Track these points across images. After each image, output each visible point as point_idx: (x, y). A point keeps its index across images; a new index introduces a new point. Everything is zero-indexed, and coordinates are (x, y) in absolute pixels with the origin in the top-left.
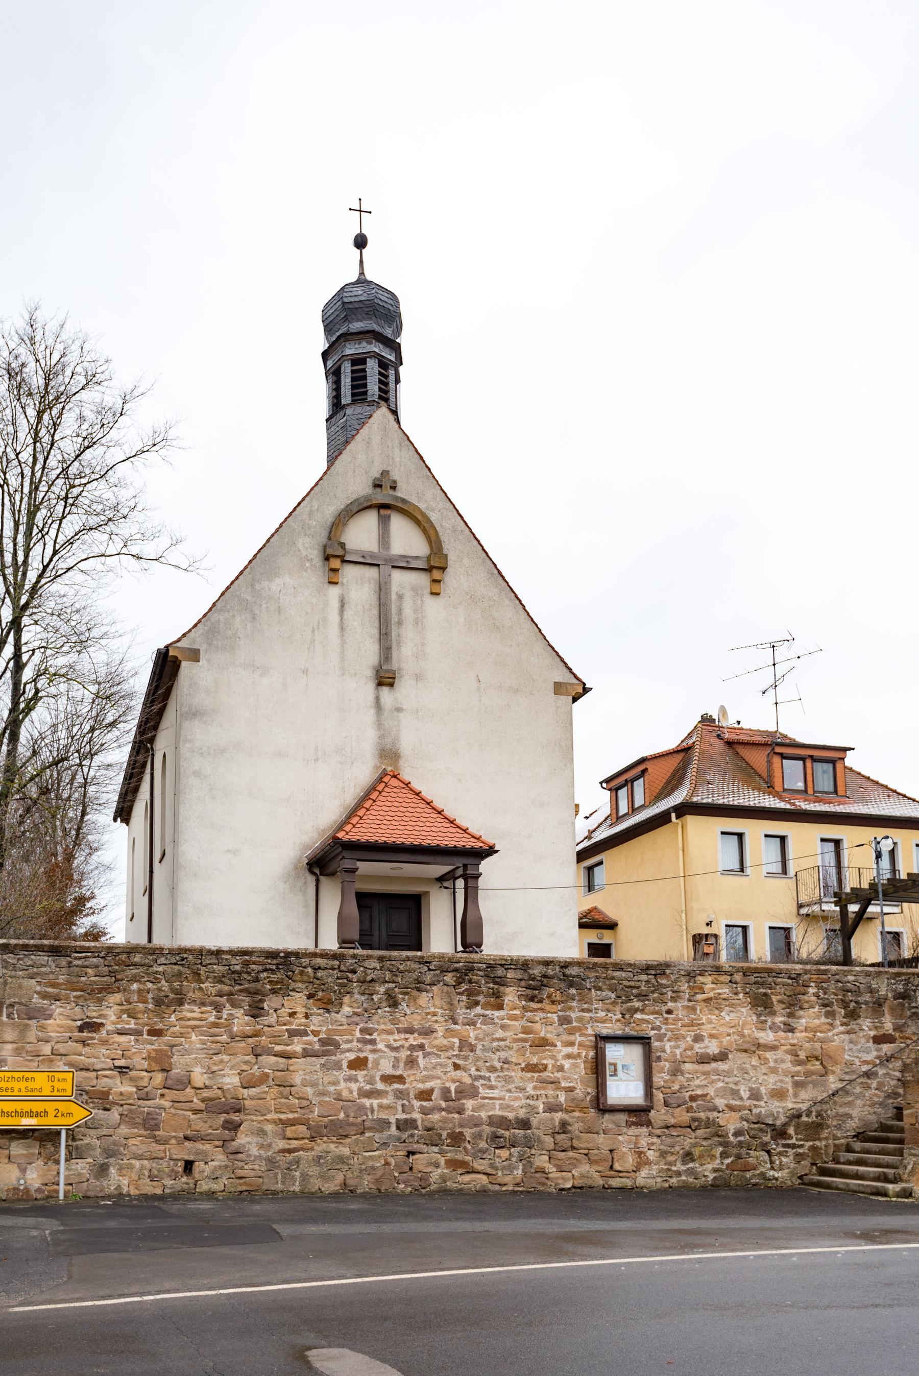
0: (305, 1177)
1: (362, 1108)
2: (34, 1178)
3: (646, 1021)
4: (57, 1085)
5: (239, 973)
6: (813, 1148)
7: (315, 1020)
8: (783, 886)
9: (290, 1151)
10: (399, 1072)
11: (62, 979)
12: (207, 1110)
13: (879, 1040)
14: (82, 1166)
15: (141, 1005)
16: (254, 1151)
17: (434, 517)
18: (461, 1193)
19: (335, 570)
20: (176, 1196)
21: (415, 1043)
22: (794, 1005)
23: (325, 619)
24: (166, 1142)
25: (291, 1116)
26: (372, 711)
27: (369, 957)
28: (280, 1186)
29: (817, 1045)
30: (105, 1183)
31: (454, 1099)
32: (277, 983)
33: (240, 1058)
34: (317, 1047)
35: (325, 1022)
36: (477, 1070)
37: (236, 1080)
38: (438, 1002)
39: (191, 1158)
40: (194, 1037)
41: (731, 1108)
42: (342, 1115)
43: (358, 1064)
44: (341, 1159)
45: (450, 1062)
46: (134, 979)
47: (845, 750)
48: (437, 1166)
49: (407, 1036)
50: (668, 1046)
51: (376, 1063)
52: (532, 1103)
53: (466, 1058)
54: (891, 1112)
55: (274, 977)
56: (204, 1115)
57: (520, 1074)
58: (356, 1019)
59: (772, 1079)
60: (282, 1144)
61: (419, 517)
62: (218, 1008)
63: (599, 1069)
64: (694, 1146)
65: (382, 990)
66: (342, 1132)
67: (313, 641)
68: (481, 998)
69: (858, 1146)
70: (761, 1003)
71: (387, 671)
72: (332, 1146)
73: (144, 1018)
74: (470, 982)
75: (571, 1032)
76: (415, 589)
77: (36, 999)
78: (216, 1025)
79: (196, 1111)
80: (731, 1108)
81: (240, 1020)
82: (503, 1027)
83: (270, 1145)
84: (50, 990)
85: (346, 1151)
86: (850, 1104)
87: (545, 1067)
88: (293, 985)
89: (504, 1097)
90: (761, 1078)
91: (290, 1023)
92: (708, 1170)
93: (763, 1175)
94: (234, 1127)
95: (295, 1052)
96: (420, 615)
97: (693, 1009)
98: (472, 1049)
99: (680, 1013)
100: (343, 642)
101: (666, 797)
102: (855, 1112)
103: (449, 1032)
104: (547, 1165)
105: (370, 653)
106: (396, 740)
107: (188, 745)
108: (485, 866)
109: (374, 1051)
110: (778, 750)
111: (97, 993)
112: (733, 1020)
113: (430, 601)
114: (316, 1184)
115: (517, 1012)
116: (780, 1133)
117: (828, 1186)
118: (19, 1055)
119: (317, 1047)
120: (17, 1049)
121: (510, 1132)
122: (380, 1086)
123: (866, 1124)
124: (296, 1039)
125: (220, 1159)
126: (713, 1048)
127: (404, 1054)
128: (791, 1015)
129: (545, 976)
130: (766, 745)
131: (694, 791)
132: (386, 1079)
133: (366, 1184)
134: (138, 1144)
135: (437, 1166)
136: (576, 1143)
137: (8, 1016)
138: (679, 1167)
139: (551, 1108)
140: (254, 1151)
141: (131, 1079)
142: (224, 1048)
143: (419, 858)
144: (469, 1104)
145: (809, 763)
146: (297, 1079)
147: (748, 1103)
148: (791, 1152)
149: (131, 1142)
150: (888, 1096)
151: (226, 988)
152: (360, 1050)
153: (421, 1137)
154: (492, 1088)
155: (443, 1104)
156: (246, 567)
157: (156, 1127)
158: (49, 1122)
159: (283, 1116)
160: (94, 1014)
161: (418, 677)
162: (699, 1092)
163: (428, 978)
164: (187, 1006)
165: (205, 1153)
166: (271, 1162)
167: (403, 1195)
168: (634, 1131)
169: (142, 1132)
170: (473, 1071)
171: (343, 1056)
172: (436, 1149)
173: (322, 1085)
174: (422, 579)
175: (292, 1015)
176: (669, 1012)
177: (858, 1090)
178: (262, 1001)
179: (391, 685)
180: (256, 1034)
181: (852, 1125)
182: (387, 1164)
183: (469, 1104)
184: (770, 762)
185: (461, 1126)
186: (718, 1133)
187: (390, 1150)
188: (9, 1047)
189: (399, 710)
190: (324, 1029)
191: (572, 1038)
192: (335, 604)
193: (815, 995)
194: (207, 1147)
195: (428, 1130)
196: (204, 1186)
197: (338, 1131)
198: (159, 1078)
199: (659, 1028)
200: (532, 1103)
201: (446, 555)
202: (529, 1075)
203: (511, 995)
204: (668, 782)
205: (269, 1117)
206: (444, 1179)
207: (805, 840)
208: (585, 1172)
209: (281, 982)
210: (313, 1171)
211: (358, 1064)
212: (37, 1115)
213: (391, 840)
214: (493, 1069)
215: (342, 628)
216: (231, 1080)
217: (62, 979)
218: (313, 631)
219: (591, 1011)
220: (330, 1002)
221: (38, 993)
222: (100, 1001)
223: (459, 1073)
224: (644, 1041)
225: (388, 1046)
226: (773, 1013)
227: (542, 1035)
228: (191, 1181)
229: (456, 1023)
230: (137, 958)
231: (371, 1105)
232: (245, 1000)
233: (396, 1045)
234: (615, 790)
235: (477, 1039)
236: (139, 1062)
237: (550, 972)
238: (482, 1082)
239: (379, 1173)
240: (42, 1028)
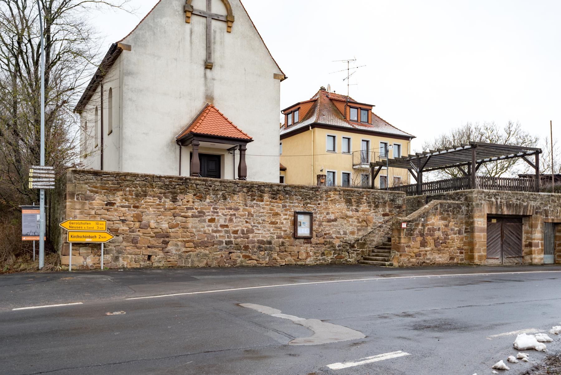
0: (193, 261)
1: (213, 236)
2: (90, 261)
3: (311, 207)
4: (100, 226)
5: (168, 185)
6: (362, 251)
8: (349, 157)
9: (187, 252)
10: (226, 224)
11: (98, 185)
12: (156, 236)
13: (384, 215)
14: (109, 257)
15: (130, 196)
16: (174, 252)
18: (247, 267)
19: (189, 17)
20: (146, 268)
22: (359, 203)
24: (141, 248)
25: (187, 239)
26: (203, 79)
27: (216, 181)
28: (183, 265)
29: (365, 216)
30: (118, 264)
31: (246, 233)
32: (182, 189)
33: (168, 217)
34: (197, 214)
35: (200, 205)
37: (167, 226)
38: (241, 198)
39: (151, 254)
41: (337, 238)
43: (212, 220)
44: (206, 255)
46: (127, 186)
47: (372, 106)
48: (239, 257)
50: (318, 216)
51: (218, 220)
53: (250, 219)
54: (386, 239)
55: (181, 187)
56: (155, 238)
57: (268, 225)
58: (211, 204)
59: (351, 228)
60: (184, 249)
62: (160, 198)
63: (295, 224)
64: (325, 250)
65: (221, 193)
66: (206, 245)
67: (179, 47)
68: (256, 197)
69: (376, 250)
70: (349, 202)
71: (209, 63)
72: (202, 250)
73: (131, 201)
74: (252, 191)
75: (286, 210)
76: (221, 29)
77: (88, 192)
78: (159, 205)
79: (152, 237)
80: (337, 238)
81: (168, 203)
82: (263, 208)
83: (180, 250)
84: (94, 189)
85: (207, 252)
86: (374, 236)
87: (277, 223)
88: (188, 191)
89: (263, 233)
90: (347, 227)
91: (187, 205)
92: (329, 259)
93: (346, 260)
94: (166, 243)
97: (327, 203)
99: (323, 205)
100: (191, 49)
101: (307, 119)
102: (375, 239)
103: (244, 210)
104: (277, 257)
105: (202, 54)
107: (126, 87)
108: (248, 145)
109: (218, 216)
110: (349, 104)
111: (113, 191)
112: (339, 207)
113: (227, 35)
114: (197, 264)
115: (268, 203)
116: (352, 246)
117: (367, 263)
118: (82, 214)
119: (197, 214)
120: (81, 212)
121: (265, 246)
122: (220, 229)
123: (379, 243)
124: (189, 211)
125: (161, 254)
126: (332, 217)
127: (228, 217)
128: (358, 206)
129: (278, 190)
130: (344, 102)
131: (318, 118)
132: (222, 226)
133: (215, 264)
134: (130, 249)
135: (239, 257)
136: (287, 249)
137: (77, 199)
138: (320, 258)
139: (279, 237)
140: (174, 252)
141: (127, 224)
142: (162, 214)
143: (224, 141)
144: (251, 235)
145: (359, 110)
146: (190, 225)
147: (343, 236)
148: (355, 252)
149: (127, 248)
150: (386, 234)
151: (163, 191)
152: (213, 215)
153: (234, 247)
154: (259, 230)
155: (242, 235)
156: (151, 12)
157: (137, 243)
158: (97, 240)
159: (184, 239)
161: (221, 67)
162: (327, 232)
163: (237, 189)
164: (148, 197)
165: (156, 253)
166: (180, 256)
167: (228, 267)
168: (306, 245)
169: (131, 244)
170: (252, 224)
172: (239, 251)
173: (199, 228)
174: (223, 25)
175: (188, 202)
176: (319, 204)
177: (377, 232)
178: (177, 196)
179: (211, 69)
180: (174, 209)
181: (375, 243)
182: (222, 256)
183: (251, 235)
184: (345, 109)
185: (248, 243)
186: (333, 246)
187: (223, 252)
188: (78, 211)
189: (214, 79)
191: (286, 213)
192: (188, 32)
193: (366, 199)
194: (156, 250)
195: (237, 244)
196: (155, 265)
197: (204, 245)
198: (137, 224)
199: (315, 210)
203: (266, 197)
204: (308, 113)
205: (179, 239)
206: (242, 262)
207: (357, 140)
208: (289, 259)
209: (184, 189)
210: (196, 259)
211: (212, 220)
212: (92, 237)
213: (213, 134)
214: (259, 223)
215: (191, 43)
216: (165, 226)
217: (98, 185)
220: (202, 197)
221: (89, 190)
222: (114, 194)
224: (310, 214)
225: (223, 214)
226: (352, 205)
228: (151, 263)
230: (128, 178)
232: (170, 196)
234: (287, 115)
236: (130, 218)
237: (280, 189)
239: (219, 260)
240: (91, 204)
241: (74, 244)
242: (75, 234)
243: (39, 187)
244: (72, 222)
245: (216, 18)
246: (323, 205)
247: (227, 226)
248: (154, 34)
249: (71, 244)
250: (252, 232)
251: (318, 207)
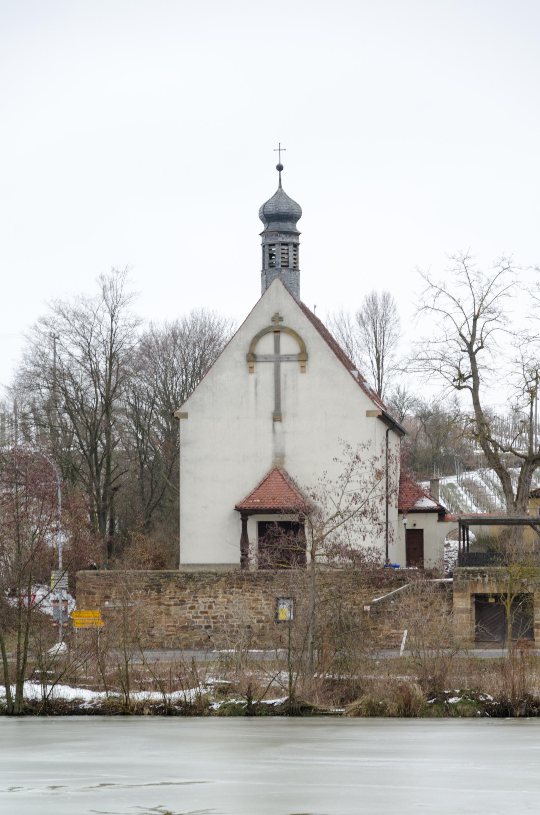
1: (193, 622)
10: (206, 610)
16: (158, 635)
34: (178, 602)
42: (186, 624)
43: (192, 608)
51: (198, 608)
62: (146, 590)
65: (200, 583)
68: (235, 586)
85: (187, 635)
105: (270, 406)
109: (198, 603)
119: (178, 602)
127: (208, 604)
132: (201, 612)
192: (252, 383)
211: (192, 608)
215: (256, 394)
223: (227, 610)
235: (233, 599)
245: (288, 358)
247: (206, 612)
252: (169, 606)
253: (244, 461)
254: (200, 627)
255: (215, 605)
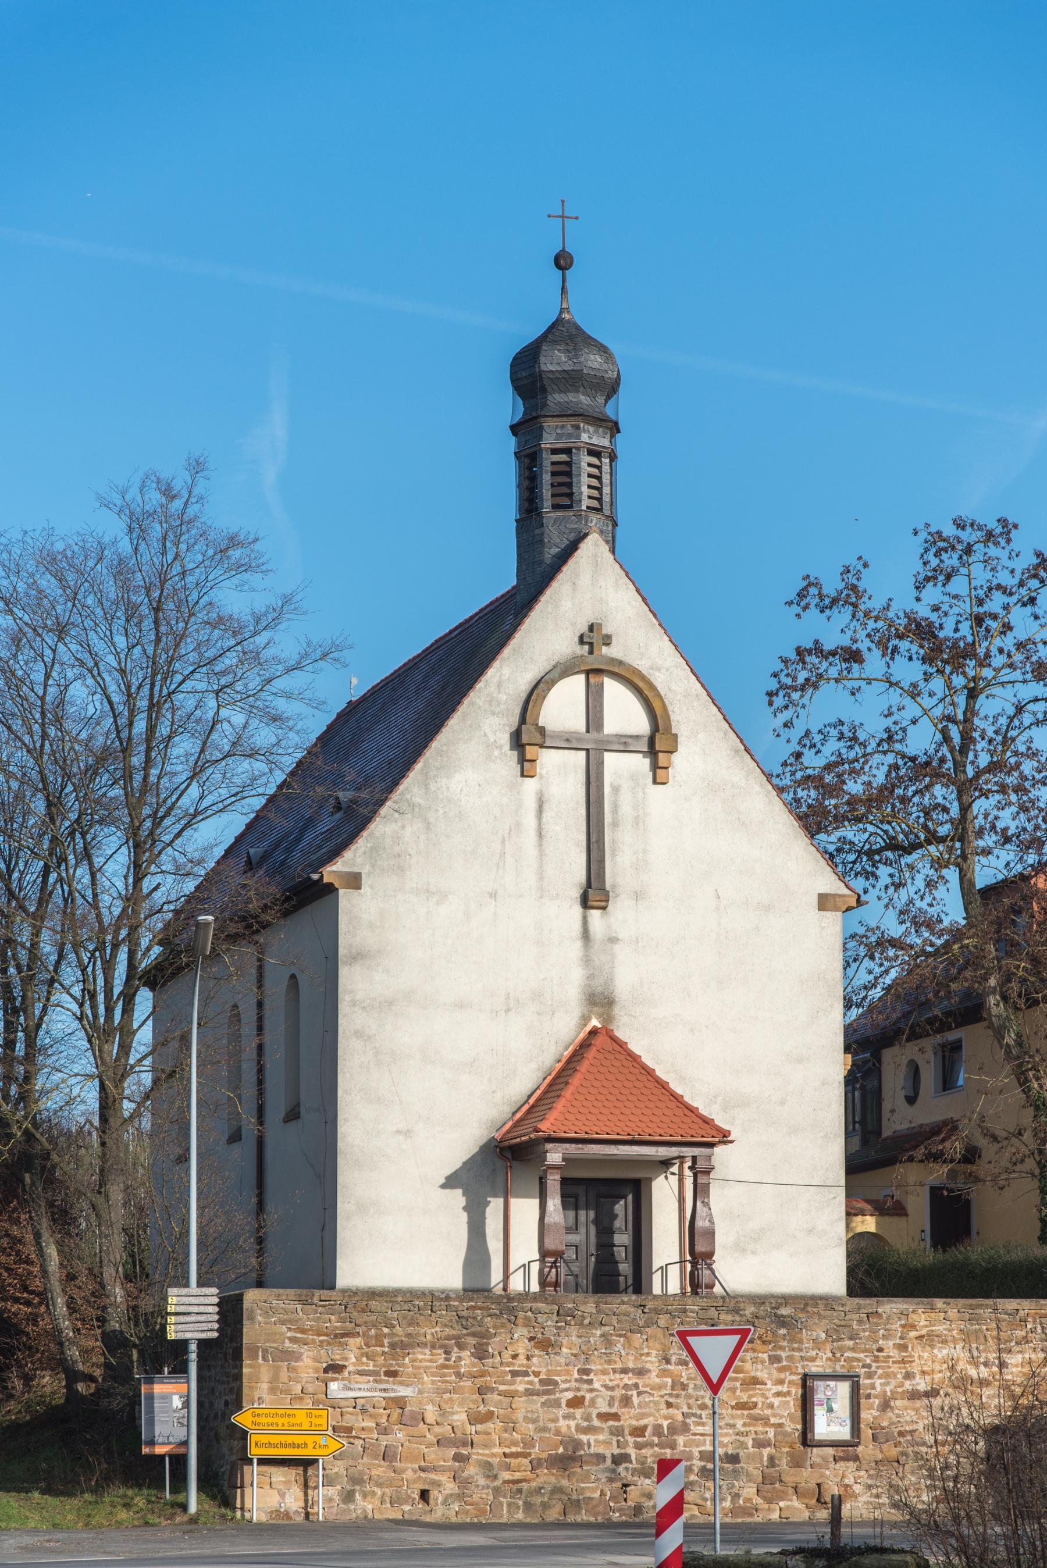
4: (315, 1421)
7: (535, 1360)
10: (613, 1410)
14: (333, 1492)
15: (378, 1349)
17: (659, 680)
21: (630, 1383)
23: (518, 824)
25: (514, 1449)
26: (579, 944)
34: (538, 1386)
36: (689, 1408)
37: (464, 1416)
40: (426, 1378)
42: (561, 1450)
43: (576, 1402)
45: (663, 1400)
49: (622, 1376)
51: (593, 1401)
52: (742, 1439)
61: (641, 684)
67: (503, 854)
77: (287, 1344)
78: (444, 1366)
84: (299, 1335)
87: (755, 1405)
91: (513, 1364)
95: (517, 1391)
96: (641, 813)
98: (684, 1387)
100: (541, 854)
103: (663, 1373)
106: (610, 980)
109: (592, 1390)
119: (538, 1386)
122: (596, 1423)
127: (618, 1393)
132: (604, 1417)
139: (760, 1444)
144: (681, 1440)
155: (656, 1440)
157: (393, 1458)
160: (338, 1357)
171: (562, 1395)
175: (515, 1357)
180: (482, 1374)
183: (681, 1440)
189: (613, 940)
190: (544, 1370)
200: (742, 1439)
201: (676, 735)
202: (739, 1412)
211: (576, 1402)
215: (540, 835)
216: (460, 1417)
218: (503, 841)
219: (801, 1350)
221: (290, 1339)
227: (753, 1374)
229: (668, 1362)
231: (588, 1441)
233: (611, 1384)
235: (688, 1379)
238: (693, 1419)
241: (262, 1462)
242: (264, 1439)
243: (188, 1335)
244: (257, 1411)
245: (624, 744)
246: (894, 1353)
248: (428, 827)
249: (255, 1461)
250: (685, 1428)
251: (876, 1359)
252: (511, 1395)
253: (508, 1010)
254: (600, 1458)
255: (639, 1394)
